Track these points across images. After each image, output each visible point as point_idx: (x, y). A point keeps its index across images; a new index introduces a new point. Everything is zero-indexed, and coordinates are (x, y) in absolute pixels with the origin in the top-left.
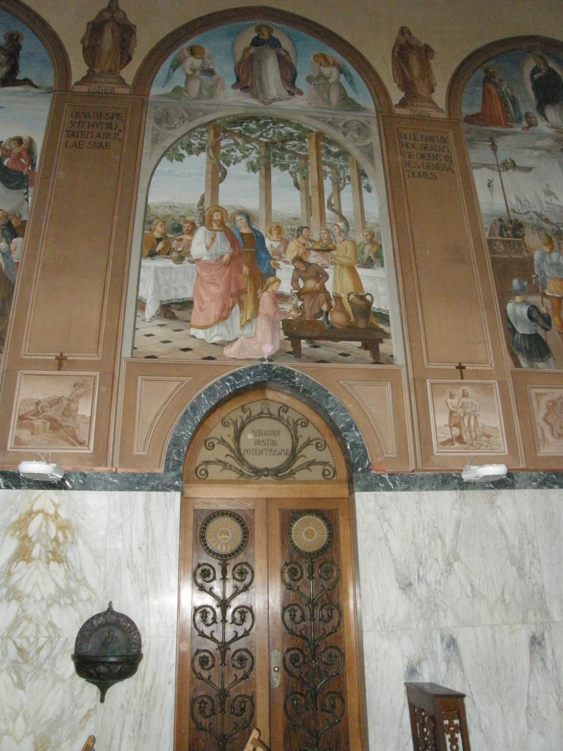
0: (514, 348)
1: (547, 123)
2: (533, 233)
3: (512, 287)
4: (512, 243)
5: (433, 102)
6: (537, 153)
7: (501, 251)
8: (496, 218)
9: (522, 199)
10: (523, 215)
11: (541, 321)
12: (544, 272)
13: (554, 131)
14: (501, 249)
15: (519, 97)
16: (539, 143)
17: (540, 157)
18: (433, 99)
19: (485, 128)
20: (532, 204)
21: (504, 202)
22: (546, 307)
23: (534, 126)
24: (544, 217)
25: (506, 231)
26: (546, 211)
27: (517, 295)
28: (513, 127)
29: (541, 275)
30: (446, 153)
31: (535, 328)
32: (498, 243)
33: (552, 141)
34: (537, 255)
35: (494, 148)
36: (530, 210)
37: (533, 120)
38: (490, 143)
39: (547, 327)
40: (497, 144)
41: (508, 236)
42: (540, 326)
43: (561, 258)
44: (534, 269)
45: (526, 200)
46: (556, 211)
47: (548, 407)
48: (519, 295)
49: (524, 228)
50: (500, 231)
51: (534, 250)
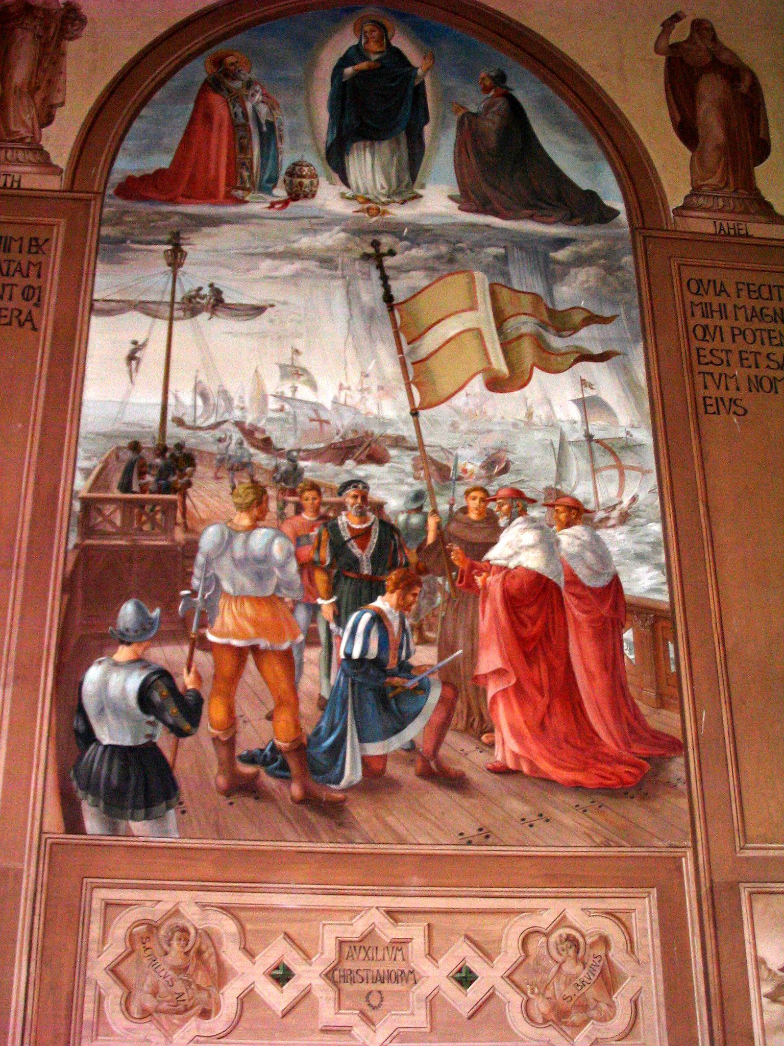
0: (75, 783)
1: (344, 189)
2: (217, 478)
3: (114, 624)
4: (148, 508)
5: (39, 150)
6: (288, 268)
7: (109, 528)
8: (124, 443)
9: (213, 389)
10: (201, 433)
11: (172, 712)
12: (218, 581)
13: (358, 207)
14: (113, 524)
15: (285, 122)
16: (305, 242)
17: (296, 276)
18: (43, 143)
19: (165, 208)
20: (236, 402)
21: (158, 399)
22: (197, 673)
23: (306, 197)
24: (258, 435)
25: (142, 474)
26: (270, 420)
27: (122, 642)
28: (247, 202)
29: (206, 589)
30: (32, 281)
31: (149, 730)
32: (108, 509)
33: (343, 235)
34: (209, 538)
35: (176, 258)
36: (226, 416)
37: (306, 182)
38: (170, 247)
39: (187, 726)
40: (185, 248)
41: (143, 490)
42: (165, 723)
43: (277, 541)
44: (192, 574)
45: (224, 393)
46: (301, 418)
47: (131, 938)
48: (129, 644)
49: (194, 465)
50: (123, 478)
51: (206, 523)
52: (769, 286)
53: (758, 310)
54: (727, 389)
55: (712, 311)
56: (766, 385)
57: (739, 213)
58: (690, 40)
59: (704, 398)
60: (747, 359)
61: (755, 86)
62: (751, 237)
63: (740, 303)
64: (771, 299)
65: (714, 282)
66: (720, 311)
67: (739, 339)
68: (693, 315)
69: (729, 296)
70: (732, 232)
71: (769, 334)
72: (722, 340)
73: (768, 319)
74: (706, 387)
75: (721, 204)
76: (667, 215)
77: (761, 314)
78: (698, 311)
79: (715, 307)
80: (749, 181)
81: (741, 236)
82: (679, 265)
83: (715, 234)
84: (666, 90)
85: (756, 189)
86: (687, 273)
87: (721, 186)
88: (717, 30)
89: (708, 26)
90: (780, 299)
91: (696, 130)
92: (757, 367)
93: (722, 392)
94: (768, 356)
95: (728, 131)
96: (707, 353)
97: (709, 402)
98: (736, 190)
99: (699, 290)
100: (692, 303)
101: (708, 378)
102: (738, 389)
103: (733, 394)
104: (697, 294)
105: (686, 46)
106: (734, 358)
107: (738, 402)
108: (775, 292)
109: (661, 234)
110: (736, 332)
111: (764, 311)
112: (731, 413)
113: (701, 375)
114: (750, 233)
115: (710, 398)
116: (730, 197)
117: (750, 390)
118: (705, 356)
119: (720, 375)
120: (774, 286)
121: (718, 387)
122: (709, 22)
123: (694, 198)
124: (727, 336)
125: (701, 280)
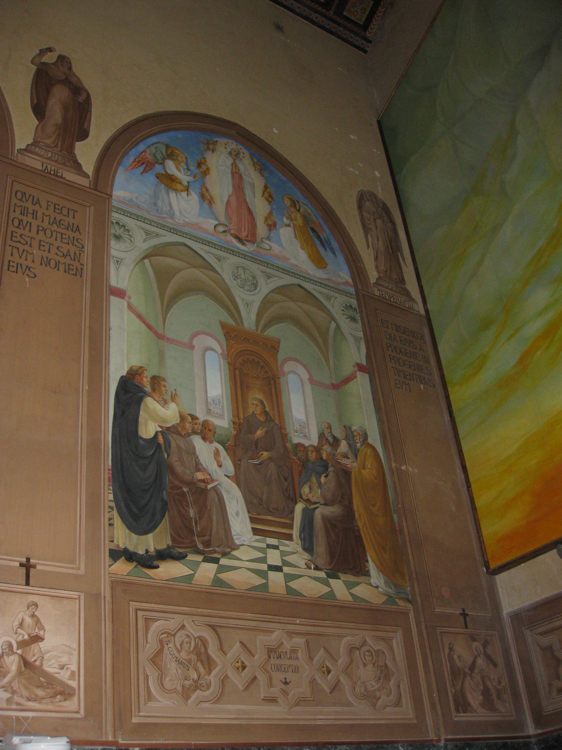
52: (69, 209)
53: (58, 220)
54: (26, 260)
55: (27, 212)
56: (53, 263)
57: (60, 163)
59: (9, 261)
60: (44, 246)
61: (88, 99)
62: (64, 178)
63: (47, 213)
64: (68, 216)
65: (34, 196)
66: (33, 214)
67: (41, 233)
68: (14, 211)
69: (41, 207)
70: (52, 172)
71: (62, 235)
72: (30, 231)
73: (63, 227)
74: (12, 255)
75: (50, 155)
76: (13, 151)
77: (60, 223)
78: (18, 210)
79: (31, 211)
80: (70, 150)
81: (57, 176)
82: (13, 181)
83: (41, 170)
84: (32, 85)
85: (74, 154)
86: (17, 187)
87: (52, 145)
88: (73, 65)
89: (69, 61)
90: (74, 218)
91: (45, 111)
92: (49, 252)
93: (22, 261)
94: (58, 248)
95: (65, 119)
96: (18, 236)
97: (11, 264)
98: (61, 151)
99: (22, 198)
100: (15, 204)
101: (15, 251)
102: (33, 261)
103: (29, 263)
104: (20, 200)
106: (35, 244)
107: (31, 269)
108: (71, 213)
109: (5, 160)
110: (41, 228)
111: (62, 222)
112: (26, 274)
113: (11, 247)
114: (64, 176)
115: (14, 262)
116: (55, 153)
117: (41, 264)
118: (16, 237)
119: (24, 250)
120: (72, 210)
121: (20, 257)
122: (69, 59)
123: (33, 147)
124: (34, 229)
125: (25, 193)
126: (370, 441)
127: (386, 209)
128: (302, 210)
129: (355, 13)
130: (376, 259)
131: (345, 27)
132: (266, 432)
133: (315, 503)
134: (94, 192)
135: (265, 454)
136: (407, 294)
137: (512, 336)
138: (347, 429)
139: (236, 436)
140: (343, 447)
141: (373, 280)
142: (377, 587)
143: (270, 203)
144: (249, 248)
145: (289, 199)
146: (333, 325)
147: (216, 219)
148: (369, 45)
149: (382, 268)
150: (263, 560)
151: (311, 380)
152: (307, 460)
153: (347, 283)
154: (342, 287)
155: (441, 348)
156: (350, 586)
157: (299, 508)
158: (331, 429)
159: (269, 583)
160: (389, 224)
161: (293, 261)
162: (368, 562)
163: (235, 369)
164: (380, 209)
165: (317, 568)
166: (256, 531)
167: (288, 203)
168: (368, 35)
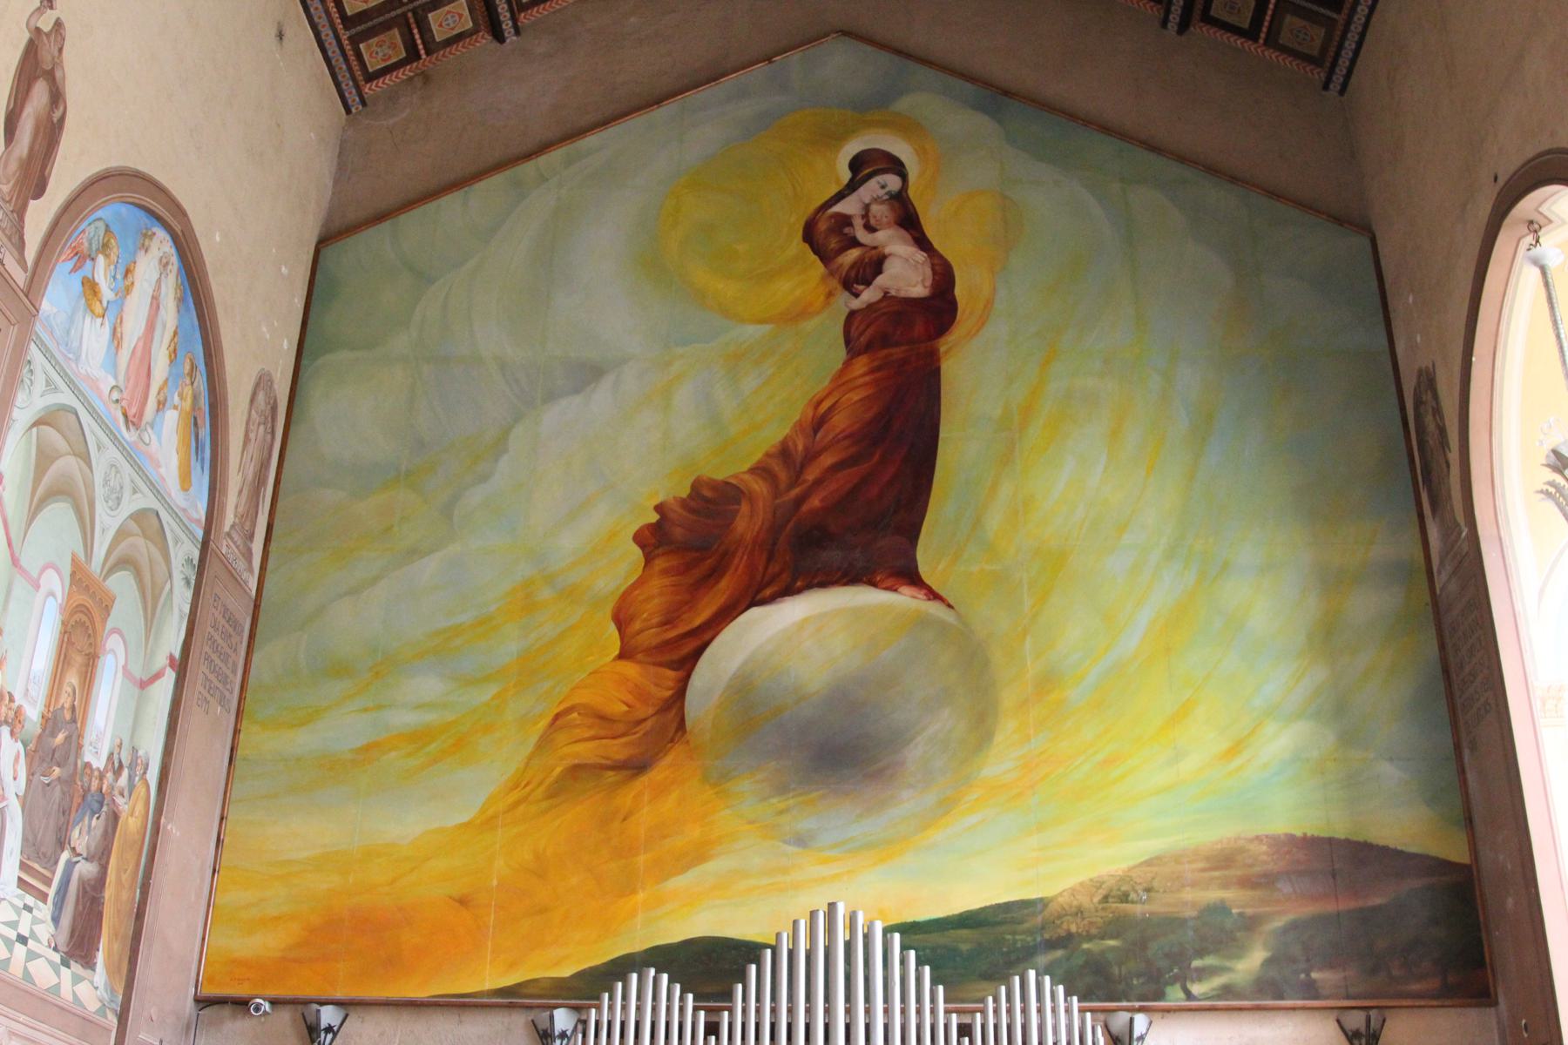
58: (48, 35)
95: (31, 149)
98: (12, 212)
105: (45, 38)
126: (148, 776)
127: (274, 409)
128: (195, 384)
129: (374, 55)
130: (241, 492)
131: (350, 69)
132: (66, 738)
133: (79, 855)
134: (21, 295)
135: (57, 771)
136: (248, 555)
137: (366, 710)
138: (134, 750)
139: (40, 737)
140: (123, 780)
141: (227, 528)
142: (96, 988)
143: (171, 362)
144: (129, 436)
145: (191, 360)
146: (168, 586)
147: (116, 378)
148: (360, 107)
149: (241, 509)
150: (13, 925)
151: (125, 668)
152: (89, 790)
153: (198, 521)
154: (193, 526)
155: (257, 658)
156: (77, 979)
157: (65, 856)
158: (121, 749)
159: (12, 959)
160: (269, 437)
161: (162, 471)
162: (98, 950)
163: (65, 632)
164: (269, 407)
165: (56, 949)
166: (22, 883)
167: (188, 367)
168: (367, 90)
